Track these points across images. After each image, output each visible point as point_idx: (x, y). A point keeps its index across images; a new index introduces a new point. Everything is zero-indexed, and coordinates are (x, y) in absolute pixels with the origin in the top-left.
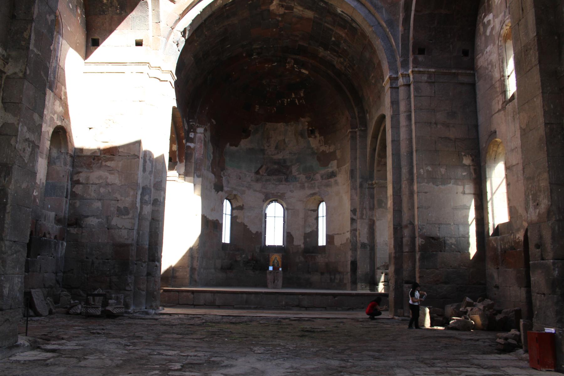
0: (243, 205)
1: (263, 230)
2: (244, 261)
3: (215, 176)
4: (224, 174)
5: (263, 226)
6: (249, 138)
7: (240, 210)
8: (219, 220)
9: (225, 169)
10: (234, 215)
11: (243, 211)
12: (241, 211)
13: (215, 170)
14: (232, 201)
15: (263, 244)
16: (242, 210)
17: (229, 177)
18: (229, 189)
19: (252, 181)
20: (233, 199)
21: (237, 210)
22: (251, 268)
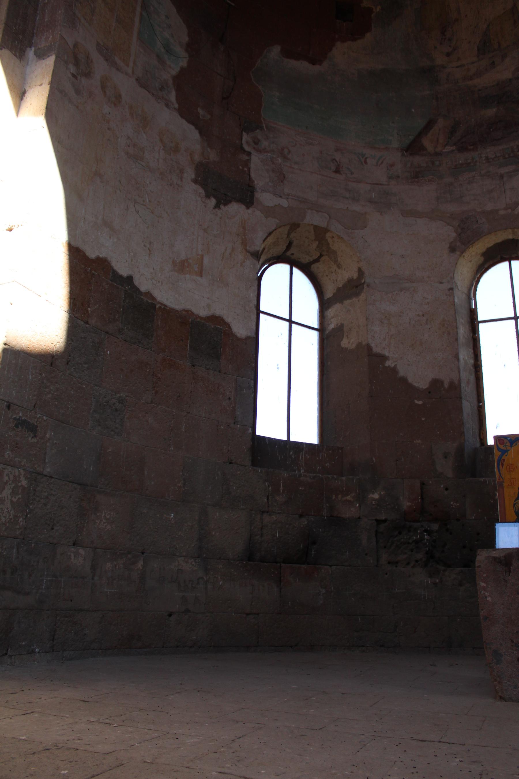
0: (360, 271)
1: (466, 376)
2: (379, 522)
3: (200, 133)
4: (256, 142)
5: (465, 355)
6: (368, 35)
7: (349, 297)
8: (228, 320)
9: (262, 128)
10: (332, 326)
11: (363, 296)
12: (355, 299)
13: (201, 111)
14: (317, 268)
15: (471, 441)
16: (357, 295)
17: (285, 158)
18: (284, 203)
19: (390, 178)
20: (317, 261)
21: (341, 302)
22: (420, 556)
